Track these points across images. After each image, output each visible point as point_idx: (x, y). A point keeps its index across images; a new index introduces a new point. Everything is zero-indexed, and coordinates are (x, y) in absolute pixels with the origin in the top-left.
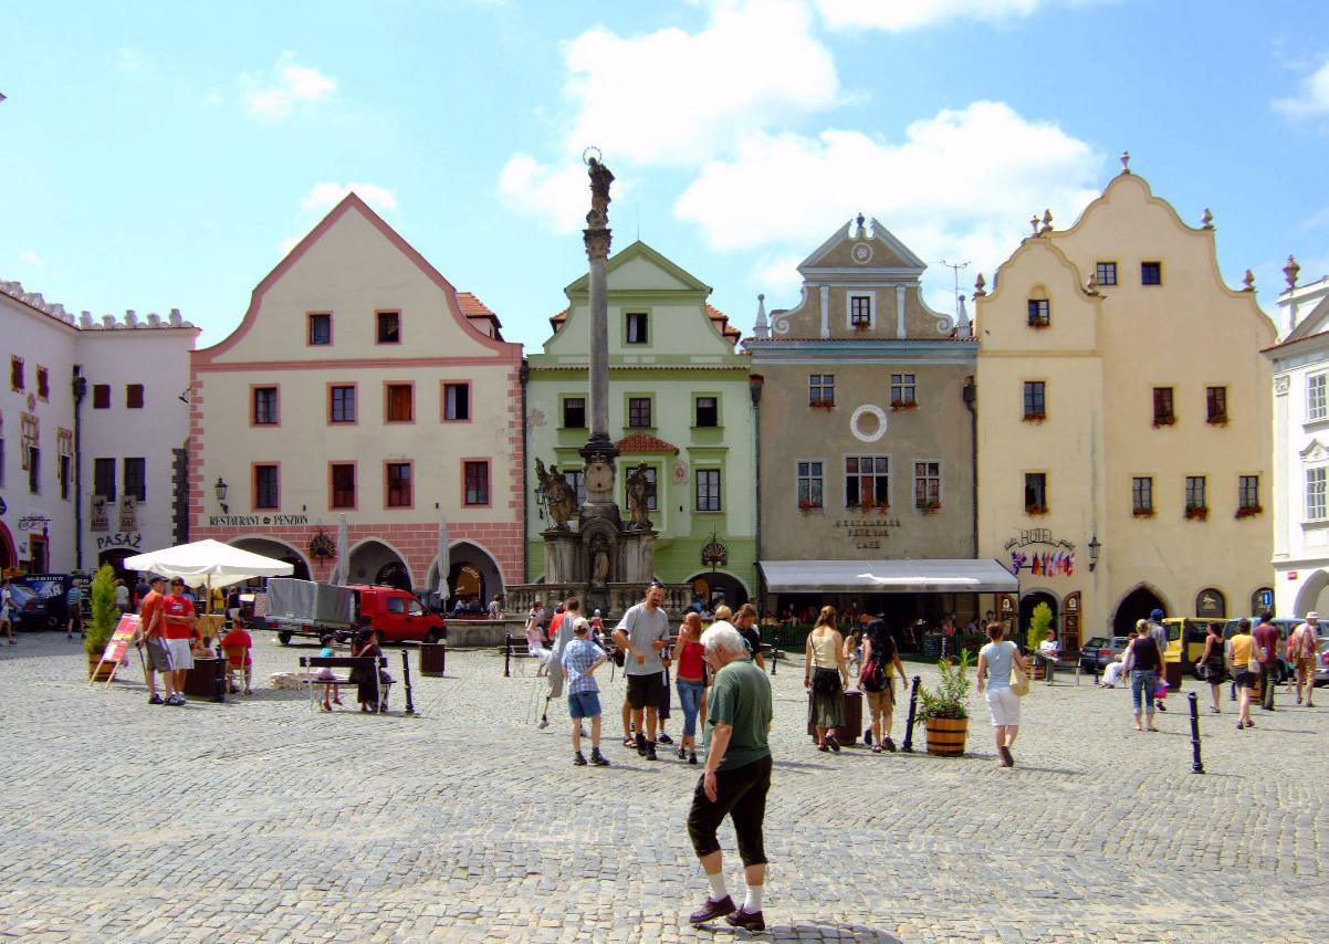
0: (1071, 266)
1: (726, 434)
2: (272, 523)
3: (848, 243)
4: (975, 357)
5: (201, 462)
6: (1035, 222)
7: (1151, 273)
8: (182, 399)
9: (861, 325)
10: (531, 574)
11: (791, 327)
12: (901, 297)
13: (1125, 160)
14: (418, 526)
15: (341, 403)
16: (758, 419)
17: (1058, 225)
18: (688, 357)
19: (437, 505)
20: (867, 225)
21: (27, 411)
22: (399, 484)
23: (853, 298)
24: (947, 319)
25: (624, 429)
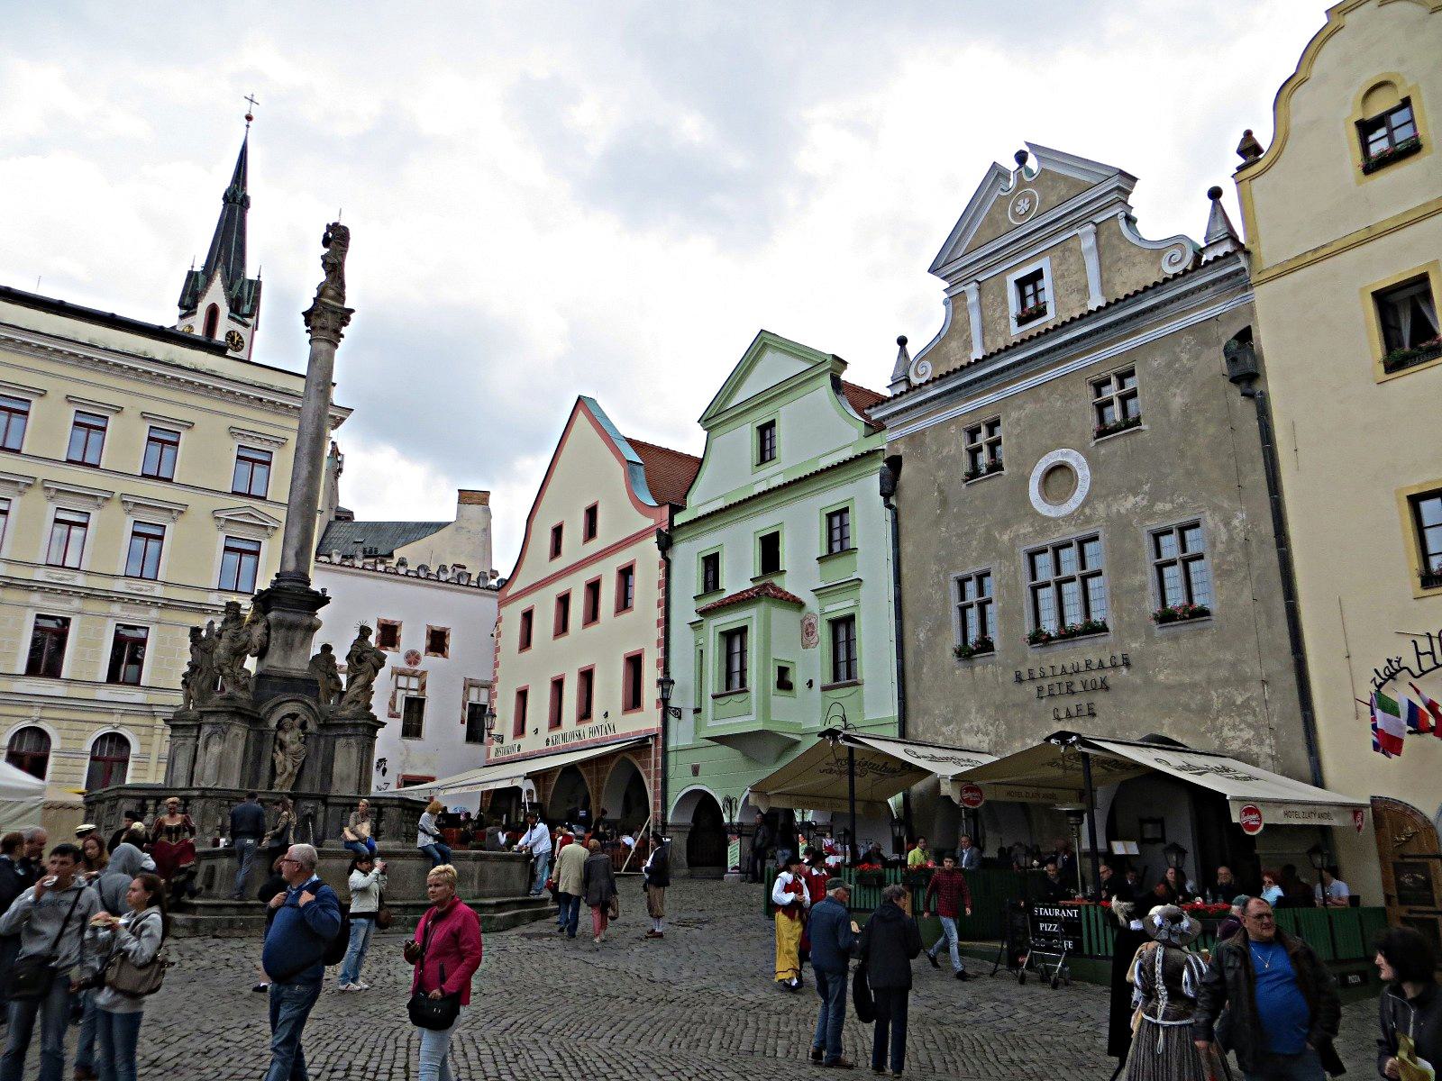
4: (1247, 287)
12: (1088, 243)
20: (1032, 163)
21: (403, 665)
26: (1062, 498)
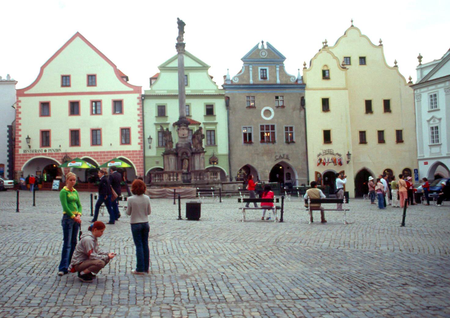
0: (335, 58)
1: (217, 117)
2: (47, 152)
3: (259, 50)
4: (305, 90)
5: (20, 130)
6: (323, 43)
7: (363, 60)
8: (13, 107)
9: (264, 78)
10: (146, 168)
12: (278, 69)
13: (352, 21)
14: (104, 152)
15: (74, 108)
17: (330, 44)
18: (202, 91)
19: (111, 145)
22: (96, 136)
23: (261, 69)
24: (294, 77)
26: (268, 117)
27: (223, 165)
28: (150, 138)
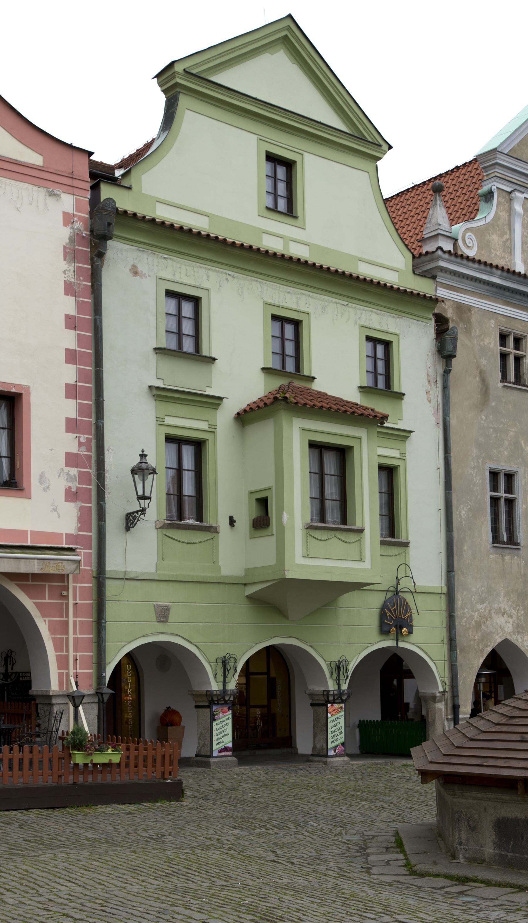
11: (479, 248)
16: (445, 388)
25: (265, 370)
27: (425, 642)
28: (141, 470)
